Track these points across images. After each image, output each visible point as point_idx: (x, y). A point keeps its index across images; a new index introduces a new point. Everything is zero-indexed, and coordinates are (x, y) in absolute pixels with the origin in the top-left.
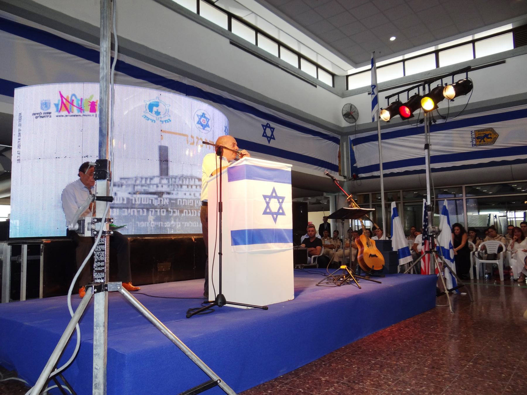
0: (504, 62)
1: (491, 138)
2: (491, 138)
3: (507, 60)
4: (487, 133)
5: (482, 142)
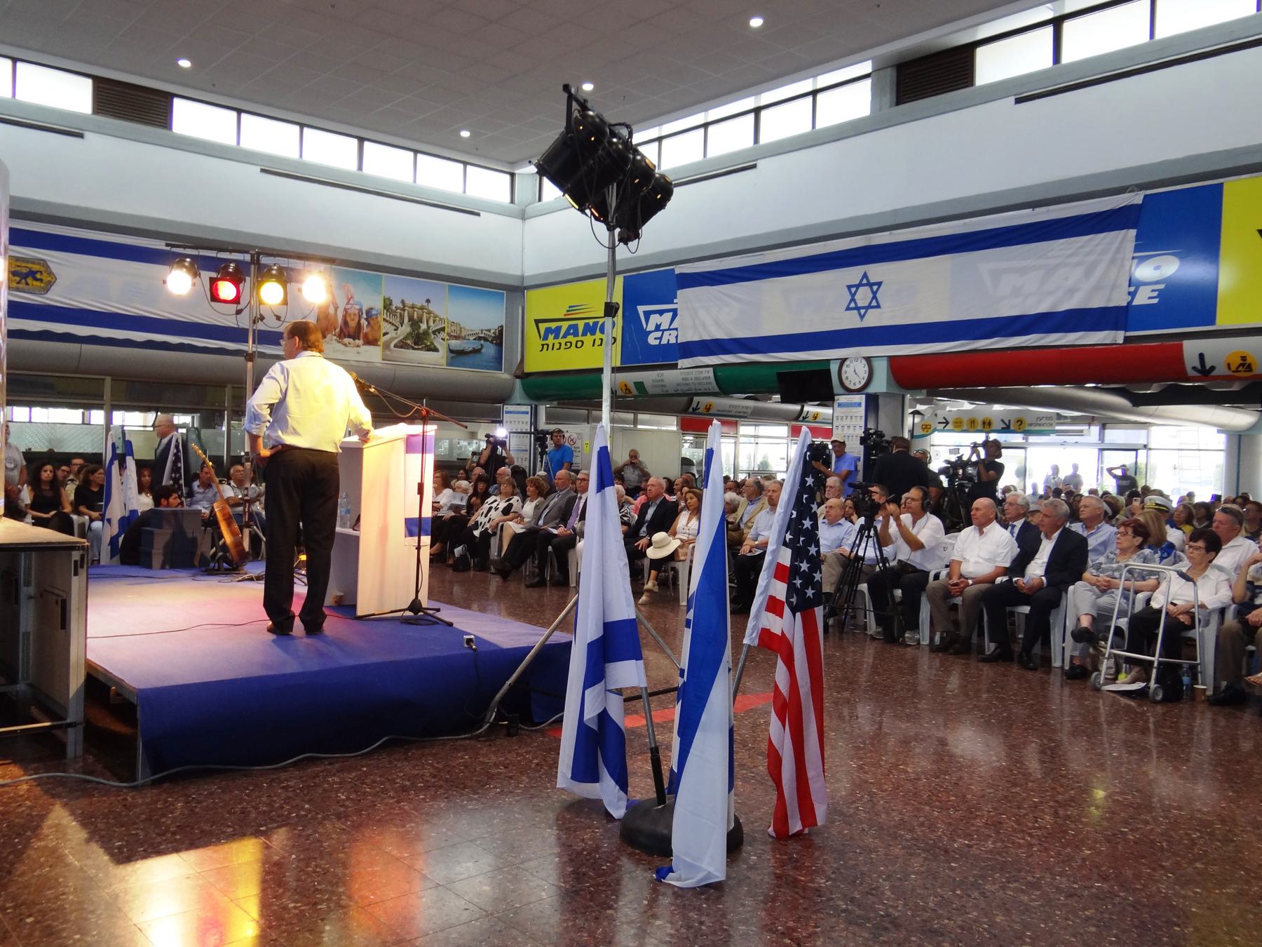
0: (81, 136)
1: (41, 280)
2: (41, 280)
3: (87, 134)
4: (35, 267)
5: (22, 286)
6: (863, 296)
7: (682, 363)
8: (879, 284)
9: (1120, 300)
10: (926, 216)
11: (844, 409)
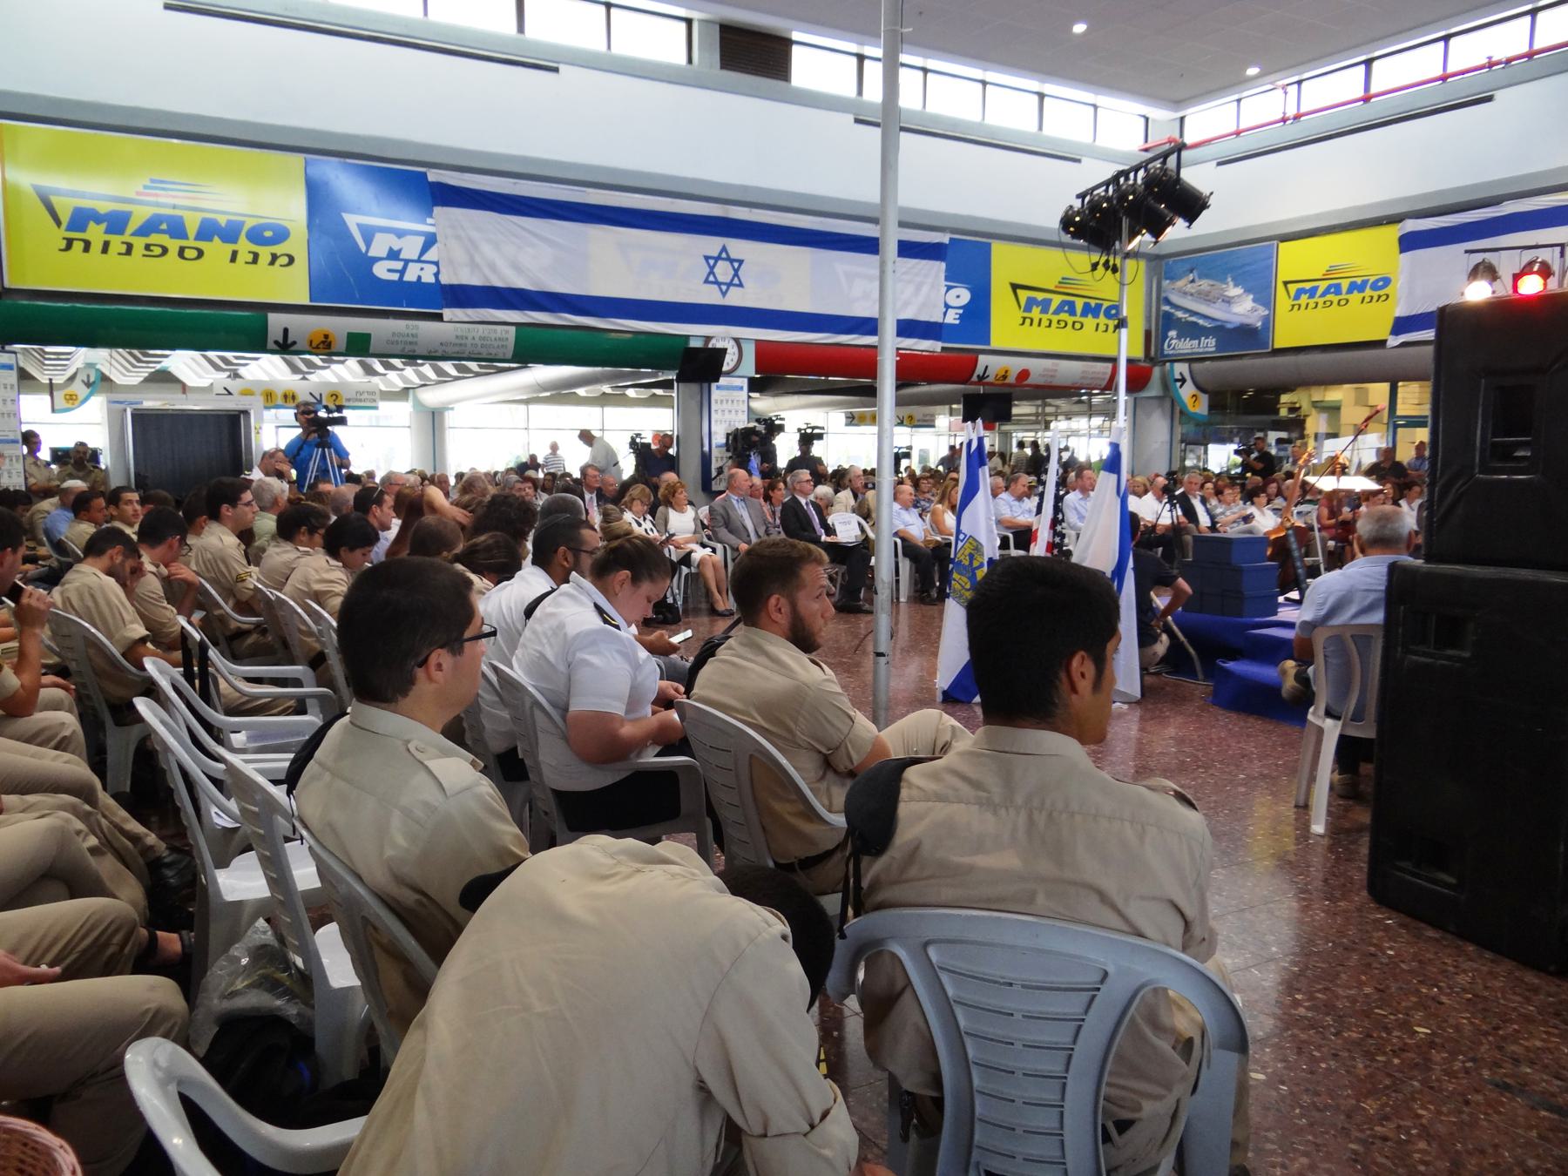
6: (723, 271)
7: (448, 313)
8: (741, 262)
9: (936, 317)
10: (697, 192)
11: (724, 393)
